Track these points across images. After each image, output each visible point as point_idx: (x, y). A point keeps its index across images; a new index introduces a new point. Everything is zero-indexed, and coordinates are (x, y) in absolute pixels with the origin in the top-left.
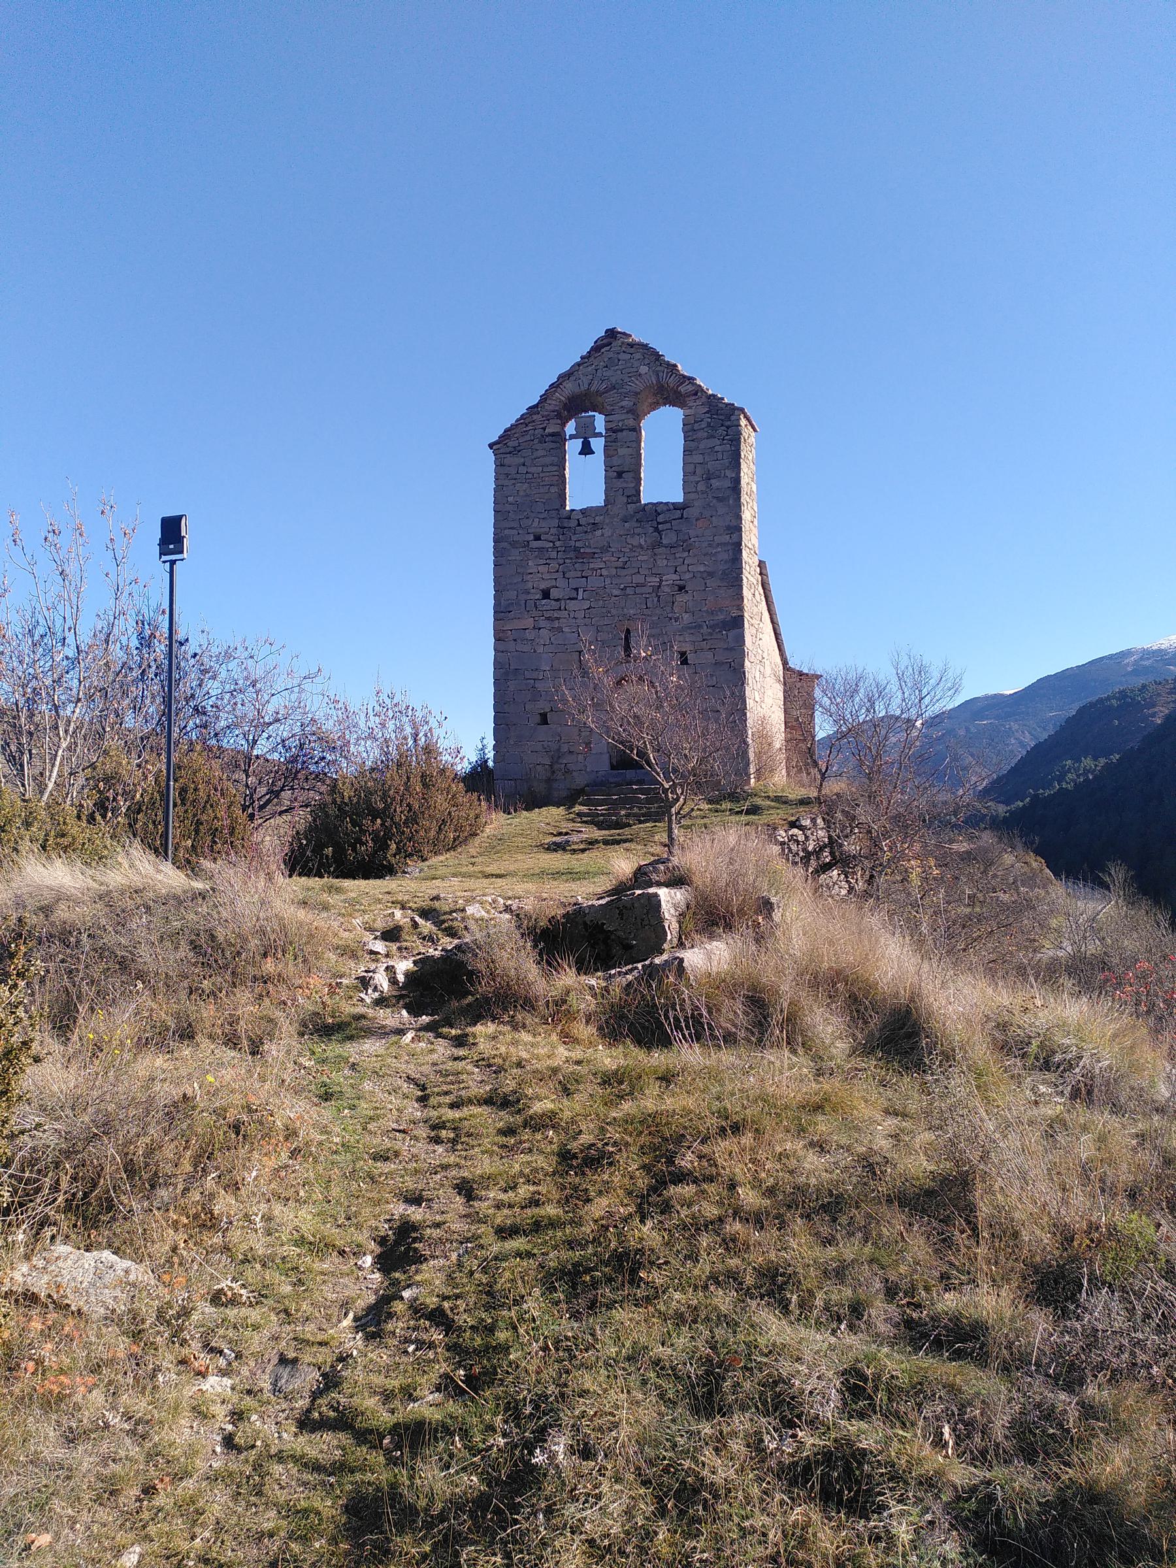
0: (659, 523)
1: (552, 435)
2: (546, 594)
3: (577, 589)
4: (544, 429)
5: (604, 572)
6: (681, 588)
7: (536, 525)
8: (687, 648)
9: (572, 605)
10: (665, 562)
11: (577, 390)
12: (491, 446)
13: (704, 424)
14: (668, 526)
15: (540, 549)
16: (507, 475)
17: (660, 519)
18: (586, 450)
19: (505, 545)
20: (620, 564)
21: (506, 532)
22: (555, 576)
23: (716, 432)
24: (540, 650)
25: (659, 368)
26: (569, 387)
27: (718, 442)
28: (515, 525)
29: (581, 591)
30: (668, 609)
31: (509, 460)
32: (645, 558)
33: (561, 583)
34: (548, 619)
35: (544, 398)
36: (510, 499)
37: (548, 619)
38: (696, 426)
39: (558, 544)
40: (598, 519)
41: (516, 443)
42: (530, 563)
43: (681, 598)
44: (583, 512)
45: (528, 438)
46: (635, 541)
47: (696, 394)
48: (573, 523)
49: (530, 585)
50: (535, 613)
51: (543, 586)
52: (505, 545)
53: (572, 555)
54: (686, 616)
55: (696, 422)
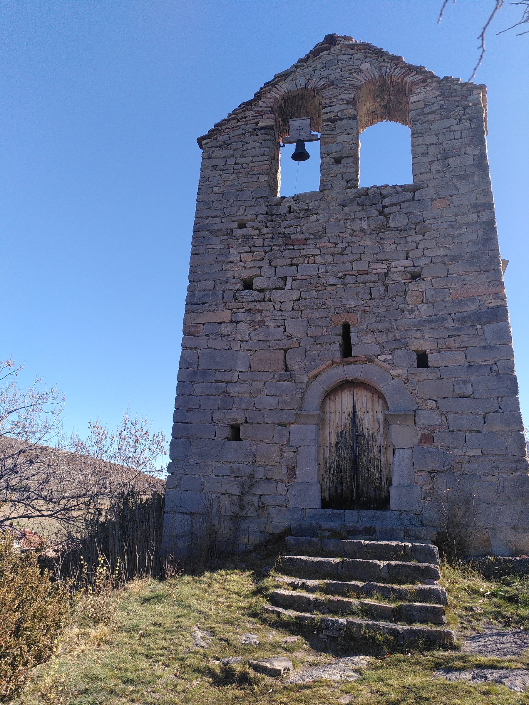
0: (384, 207)
1: (265, 128)
2: (248, 285)
3: (285, 279)
4: (257, 124)
5: (318, 259)
6: (415, 276)
7: (242, 213)
8: (425, 346)
9: (277, 295)
10: (394, 246)
11: (293, 88)
12: (200, 140)
13: (435, 107)
14: (396, 208)
15: (245, 237)
16: (214, 167)
17: (386, 202)
18: (300, 155)
19: (205, 233)
20: (337, 250)
21: (209, 221)
22: (260, 264)
23: (449, 117)
24: (237, 346)
25: (382, 64)
26: (285, 87)
27: (455, 122)
28: (219, 213)
29: (289, 281)
30: (399, 299)
31: (218, 152)
32: (369, 243)
33: (267, 271)
34: (249, 311)
35: (258, 96)
36: (216, 189)
37: (249, 311)
38: (427, 110)
39: (265, 231)
40: (312, 205)
41: (226, 138)
42: (232, 251)
43: (414, 287)
44: (296, 199)
45: (239, 132)
46: (356, 225)
47: (425, 81)
48: (283, 210)
49: (230, 274)
50: (233, 305)
51: (246, 274)
52: (205, 233)
53: (281, 241)
54: (423, 308)
55: (425, 106)
